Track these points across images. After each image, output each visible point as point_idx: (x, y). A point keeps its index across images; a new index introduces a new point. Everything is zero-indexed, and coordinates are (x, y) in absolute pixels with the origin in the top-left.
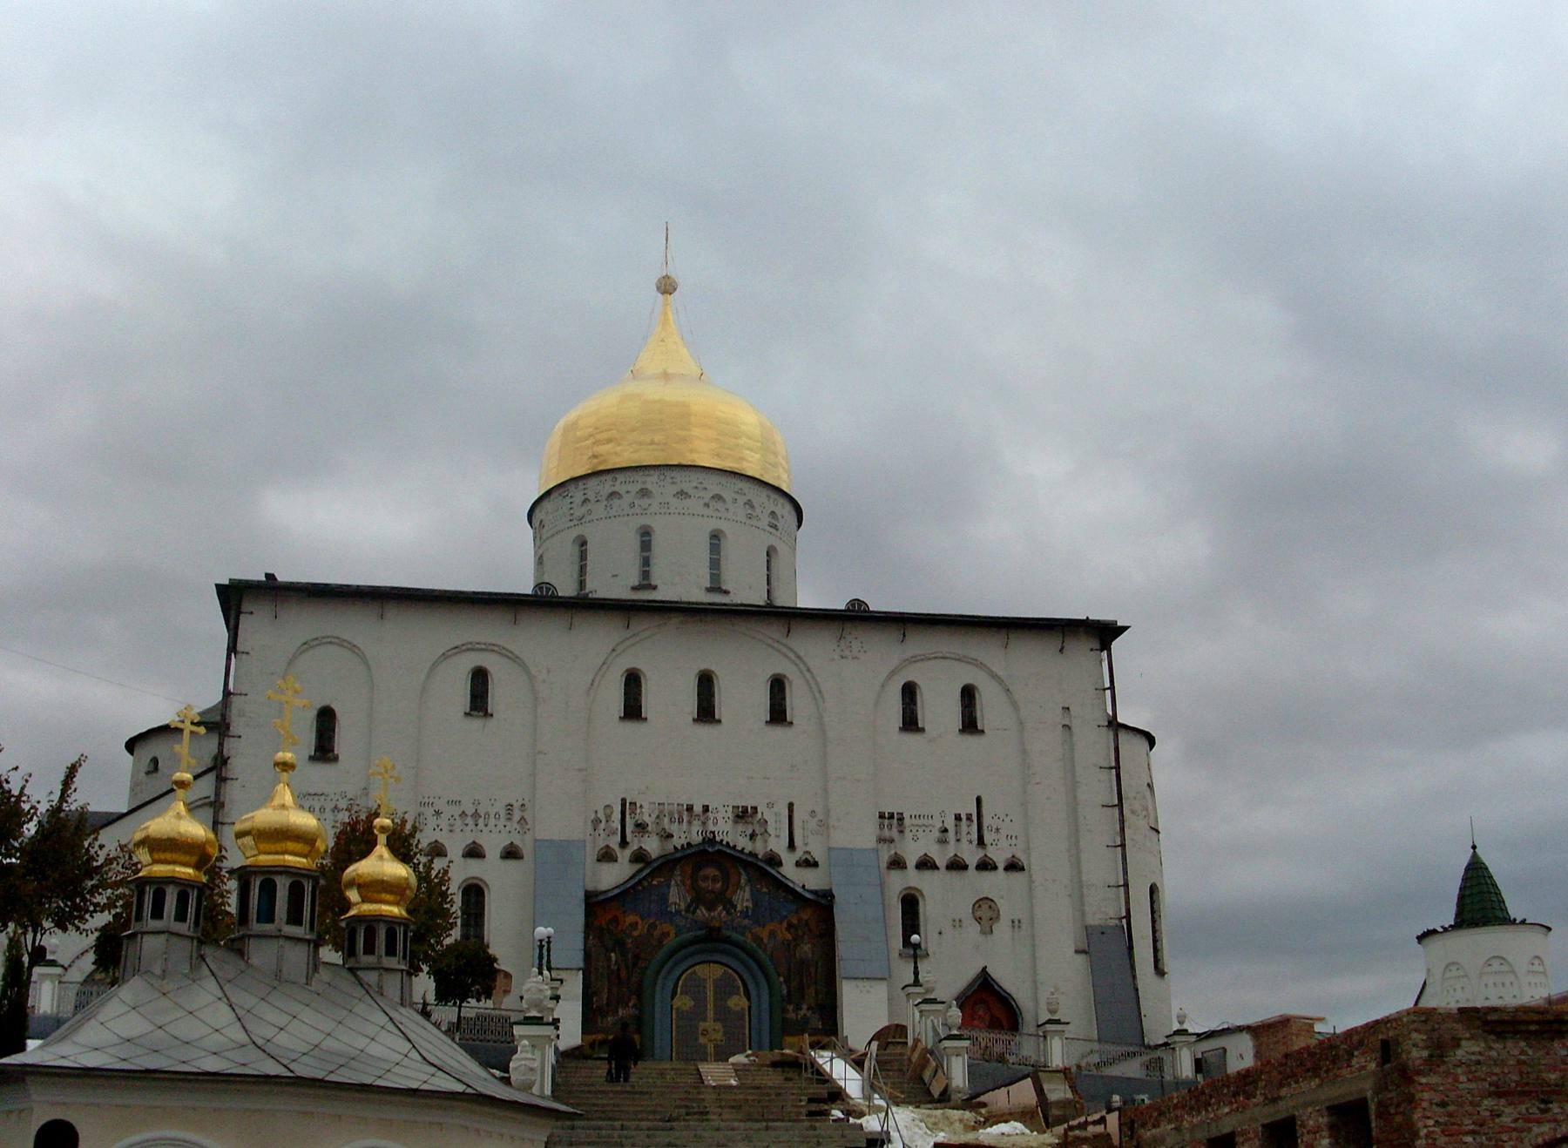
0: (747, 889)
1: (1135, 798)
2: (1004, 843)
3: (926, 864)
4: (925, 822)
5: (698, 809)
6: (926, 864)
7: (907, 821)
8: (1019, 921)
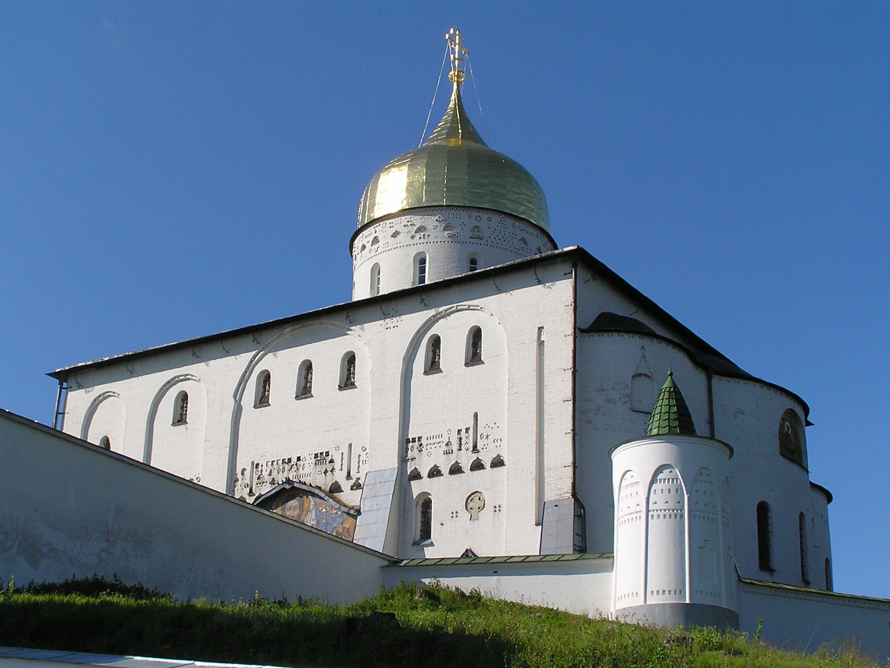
0: (314, 512)
1: (613, 389)
2: (492, 446)
3: (435, 472)
4: (438, 440)
5: (294, 460)
6: (435, 472)
7: (424, 442)
8: (500, 506)
